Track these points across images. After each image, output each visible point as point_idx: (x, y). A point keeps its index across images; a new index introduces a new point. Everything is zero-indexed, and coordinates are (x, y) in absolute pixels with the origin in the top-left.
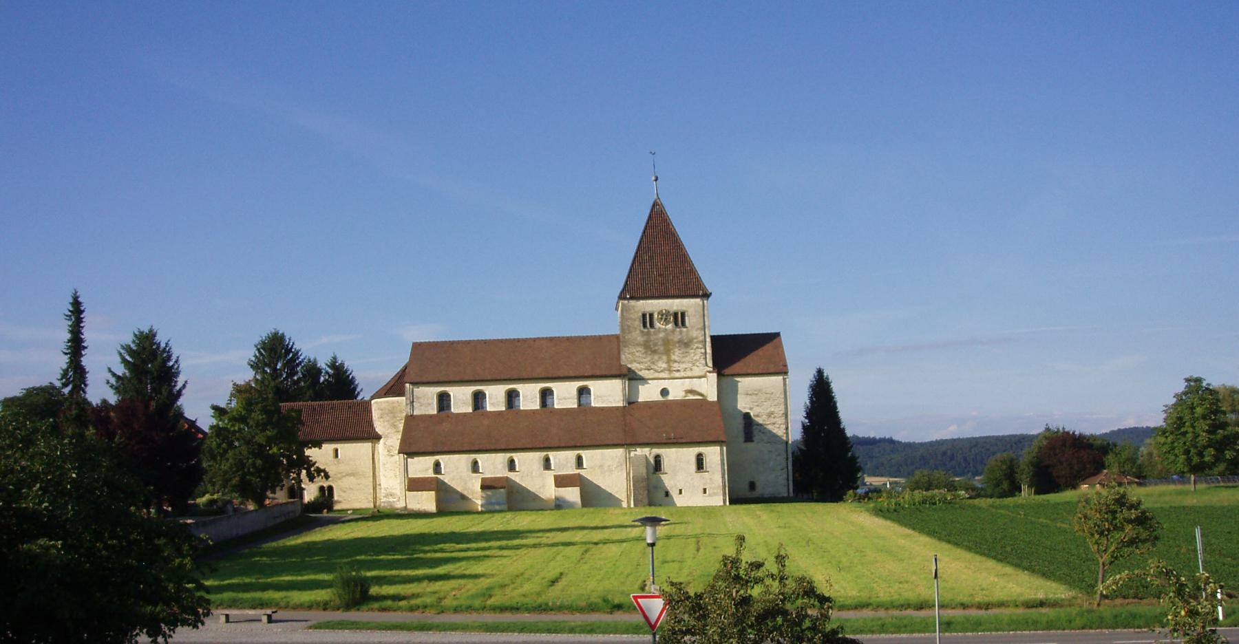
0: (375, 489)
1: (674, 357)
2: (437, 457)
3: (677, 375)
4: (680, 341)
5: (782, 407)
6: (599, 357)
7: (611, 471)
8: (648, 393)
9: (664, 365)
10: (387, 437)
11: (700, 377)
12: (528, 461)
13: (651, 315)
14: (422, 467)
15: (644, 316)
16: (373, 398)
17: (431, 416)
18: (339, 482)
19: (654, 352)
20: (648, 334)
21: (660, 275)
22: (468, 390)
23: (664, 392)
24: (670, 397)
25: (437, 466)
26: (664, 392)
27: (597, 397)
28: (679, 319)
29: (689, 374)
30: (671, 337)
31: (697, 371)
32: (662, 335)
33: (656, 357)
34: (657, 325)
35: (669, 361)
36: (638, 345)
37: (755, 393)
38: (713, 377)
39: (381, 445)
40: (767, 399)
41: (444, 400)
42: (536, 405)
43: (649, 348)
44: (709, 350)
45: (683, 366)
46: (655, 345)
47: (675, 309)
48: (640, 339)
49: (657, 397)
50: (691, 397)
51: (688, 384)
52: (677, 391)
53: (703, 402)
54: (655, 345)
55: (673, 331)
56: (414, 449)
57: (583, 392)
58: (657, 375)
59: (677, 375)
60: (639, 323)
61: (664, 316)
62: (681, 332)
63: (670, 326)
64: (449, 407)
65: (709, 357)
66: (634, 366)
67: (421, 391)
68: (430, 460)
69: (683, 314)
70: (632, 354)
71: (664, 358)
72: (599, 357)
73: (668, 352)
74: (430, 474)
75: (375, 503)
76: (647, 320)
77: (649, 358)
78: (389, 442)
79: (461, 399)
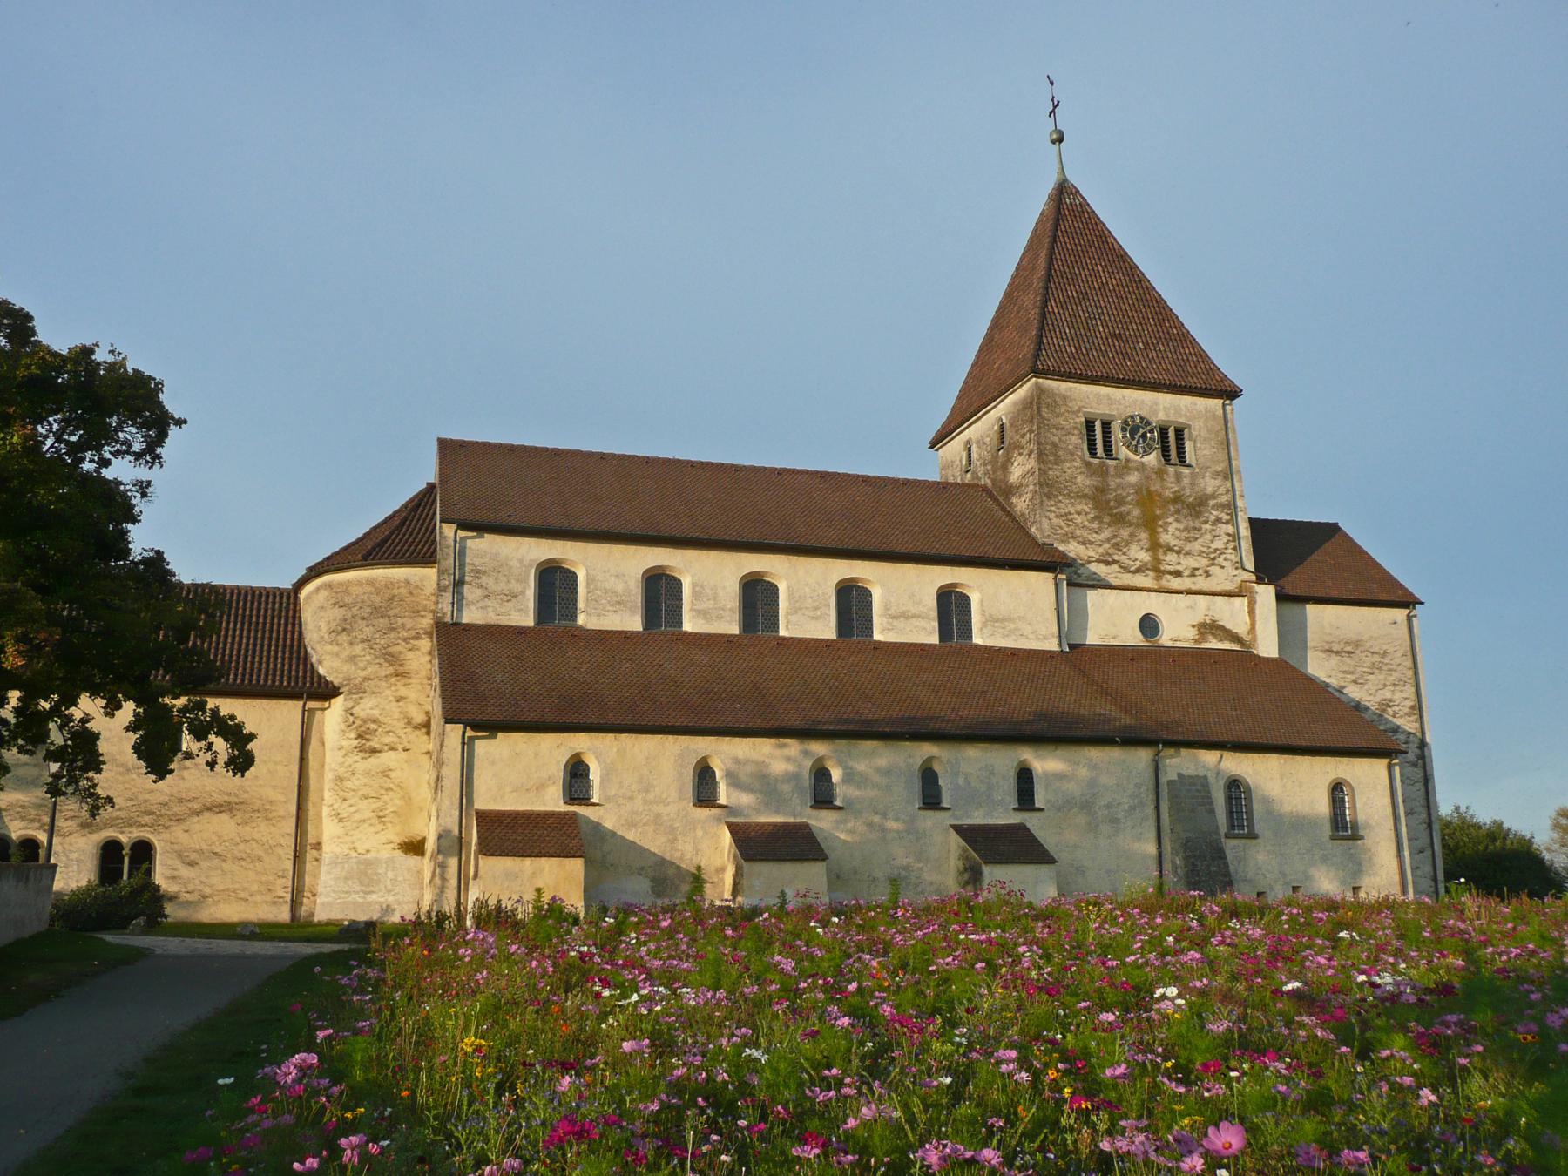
0: (298, 858)
1: (1166, 538)
2: (581, 742)
3: (1175, 583)
4: (1177, 499)
5: (1410, 691)
6: (962, 527)
7: (1114, 821)
8: (1111, 620)
9: (1144, 556)
10: (359, 691)
11: (1229, 594)
12: (871, 772)
13: (1106, 426)
14: (519, 773)
15: (1090, 424)
16: (314, 572)
17: (521, 631)
18: (178, 832)
19: (1120, 520)
20: (1103, 472)
21: (1114, 336)
22: (637, 561)
23: (1149, 625)
24: (1165, 639)
25: (576, 772)
26: (1149, 625)
27: (991, 621)
28: (1171, 442)
29: (1201, 583)
30: (1155, 487)
31: (1225, 577)
32: (1133, 478)
33: (1124, 533)
34: (1123, 452)
35: (1154, 546)
36: (1081, 496)
37: (1344, 650)
38: (1266, 594)
39: (332, 716)
40: (1375, 668)
41: (555, 586)
42: (825, 628)
43: (1106, 507)
44: (1245, 531)
45: (1188, 563)
46: (1120, 501)
47: (1161, 416)
48: (1084, 482)
49: (1132, 637)
50: (1213, 644)
51: (1203, 608)
52: (1179, 626)
53: (1245, 659)
54: (1120, 501)
55: (1160, 473)
56: (492, 713)
57: (952, 606)
58: (1127, 579)
59: (1175, 583)
60: (1077, 441)
61: (1136, 429)
62: (1178, 477)
63: (1152, 459)
64: (570, 610)
65: (1246, 546)
66: (1072, 549)
67: (483, 547)
68: (553, 750)
69: (1179, 433)
70: (1065, 516)
71: (1143, 536)
72: (962, 527)
73: (1151, 524)
74: (553, 801)
75: (295, 904)
76: (1097, 434)
77: (1106, 534)
78: (366, 707)
79: (609, 584)
